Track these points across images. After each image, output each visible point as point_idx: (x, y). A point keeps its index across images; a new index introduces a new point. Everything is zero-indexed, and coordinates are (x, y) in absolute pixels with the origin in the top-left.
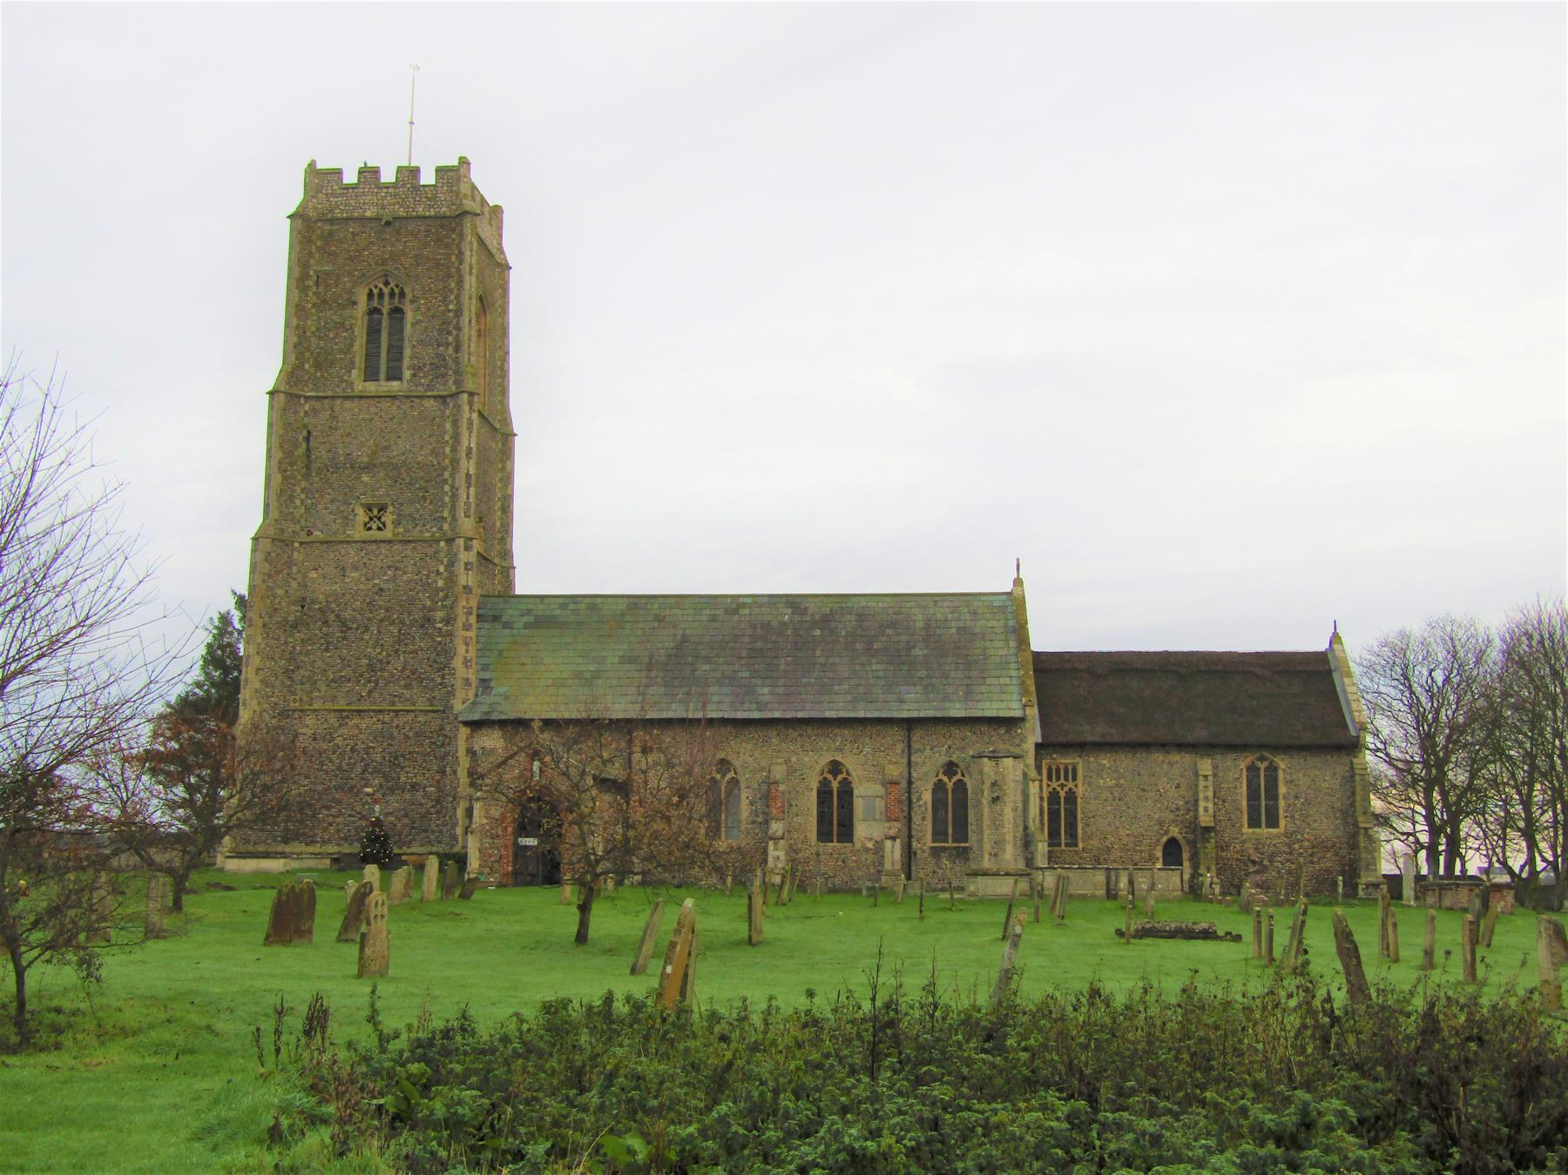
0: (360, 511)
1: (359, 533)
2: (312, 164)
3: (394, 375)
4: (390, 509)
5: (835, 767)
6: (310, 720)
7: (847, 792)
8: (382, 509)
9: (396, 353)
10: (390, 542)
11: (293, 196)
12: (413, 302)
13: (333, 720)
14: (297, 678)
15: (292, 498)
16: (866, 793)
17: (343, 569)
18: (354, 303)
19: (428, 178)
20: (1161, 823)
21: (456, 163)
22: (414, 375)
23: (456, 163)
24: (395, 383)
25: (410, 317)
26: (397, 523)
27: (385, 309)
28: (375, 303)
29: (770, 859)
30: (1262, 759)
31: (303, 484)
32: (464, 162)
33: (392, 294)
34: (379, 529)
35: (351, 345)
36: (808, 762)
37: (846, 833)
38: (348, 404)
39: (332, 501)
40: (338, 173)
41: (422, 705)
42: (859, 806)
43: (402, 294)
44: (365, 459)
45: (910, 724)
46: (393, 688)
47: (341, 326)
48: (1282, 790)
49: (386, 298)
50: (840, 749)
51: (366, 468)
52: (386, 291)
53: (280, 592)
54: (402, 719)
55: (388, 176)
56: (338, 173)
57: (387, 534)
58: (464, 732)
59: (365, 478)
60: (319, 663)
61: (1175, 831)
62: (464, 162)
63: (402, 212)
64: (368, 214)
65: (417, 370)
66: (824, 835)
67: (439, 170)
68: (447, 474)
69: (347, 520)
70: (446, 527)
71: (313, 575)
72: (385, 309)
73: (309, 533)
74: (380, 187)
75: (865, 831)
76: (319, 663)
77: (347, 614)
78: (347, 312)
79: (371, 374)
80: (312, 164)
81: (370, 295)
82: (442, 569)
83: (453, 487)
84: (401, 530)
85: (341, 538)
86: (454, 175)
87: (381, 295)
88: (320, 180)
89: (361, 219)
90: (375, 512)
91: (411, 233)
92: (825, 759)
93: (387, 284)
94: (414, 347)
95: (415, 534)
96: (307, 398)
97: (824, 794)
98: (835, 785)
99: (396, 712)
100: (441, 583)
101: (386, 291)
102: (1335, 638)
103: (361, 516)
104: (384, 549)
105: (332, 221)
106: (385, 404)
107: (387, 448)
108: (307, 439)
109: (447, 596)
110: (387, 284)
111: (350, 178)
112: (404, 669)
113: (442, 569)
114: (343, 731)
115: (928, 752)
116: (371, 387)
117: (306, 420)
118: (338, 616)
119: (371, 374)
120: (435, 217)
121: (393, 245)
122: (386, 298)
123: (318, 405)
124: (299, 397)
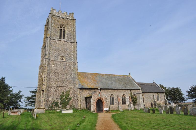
0: (60, 57)
1: (60, 60)
5: (124, 95)
6: (53, 88)
7: (125, 98)
8: (63, 57)
9: (64, 35)
13: (57, 88)
15: (50, 53)
16: (127, 98)
24: (64, 40)
25: (66, 31)
26: (65, 59)
33: (63, 28)
36: (121, 94)
37: (125, 104)
38: (58, 41)
41: (70, 86)
42: (126, 100)
43: (65, 28)
46: (66, 83)
47: (56, 30)
52: (63, 27)
57: (64, 61)
58: (79, 90)
59: (61, 52)
60: (54, 79)
61: (152, 102)
62: (73, 13)
63: (65, 17)
66: (123, 104)
68: (73, 53)
69: (58, 58)
71: (53, 65)
75: (128, 103)
77: (58, 72)
79: (60, 38)
81: (60, 27)
83: (74, 55)
85: (57, 60)
87: (62, 27)
90: (62, 57)
92: (123, 94)
95: (68, 61)
97: (123, 98)
100: (72, 68)
101: (63, 27)
104: (64, 62)
110: (63, 26)
114: (59, 90)
123: (53, 40)
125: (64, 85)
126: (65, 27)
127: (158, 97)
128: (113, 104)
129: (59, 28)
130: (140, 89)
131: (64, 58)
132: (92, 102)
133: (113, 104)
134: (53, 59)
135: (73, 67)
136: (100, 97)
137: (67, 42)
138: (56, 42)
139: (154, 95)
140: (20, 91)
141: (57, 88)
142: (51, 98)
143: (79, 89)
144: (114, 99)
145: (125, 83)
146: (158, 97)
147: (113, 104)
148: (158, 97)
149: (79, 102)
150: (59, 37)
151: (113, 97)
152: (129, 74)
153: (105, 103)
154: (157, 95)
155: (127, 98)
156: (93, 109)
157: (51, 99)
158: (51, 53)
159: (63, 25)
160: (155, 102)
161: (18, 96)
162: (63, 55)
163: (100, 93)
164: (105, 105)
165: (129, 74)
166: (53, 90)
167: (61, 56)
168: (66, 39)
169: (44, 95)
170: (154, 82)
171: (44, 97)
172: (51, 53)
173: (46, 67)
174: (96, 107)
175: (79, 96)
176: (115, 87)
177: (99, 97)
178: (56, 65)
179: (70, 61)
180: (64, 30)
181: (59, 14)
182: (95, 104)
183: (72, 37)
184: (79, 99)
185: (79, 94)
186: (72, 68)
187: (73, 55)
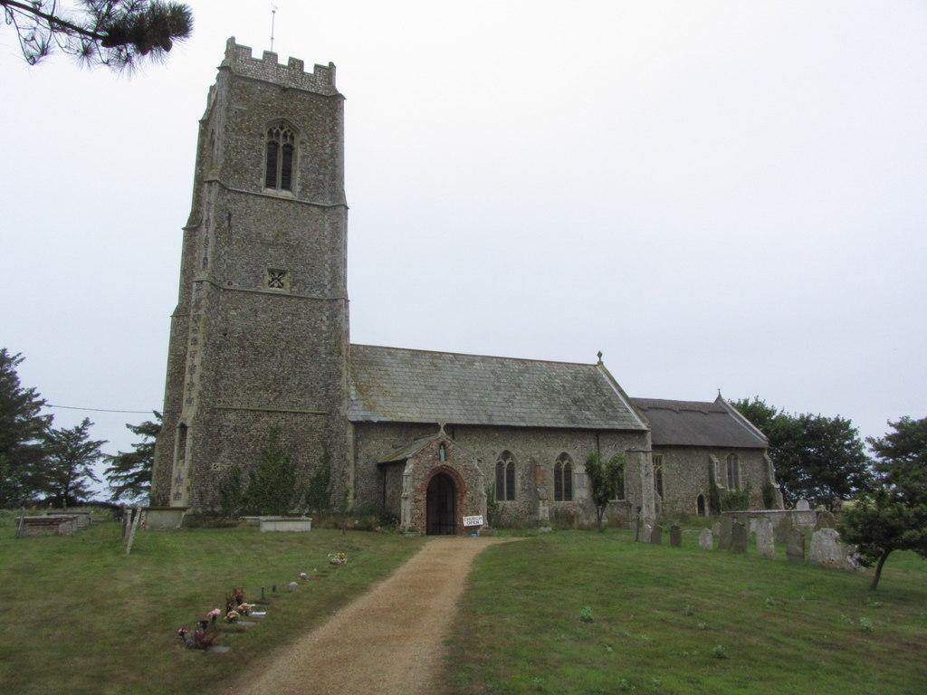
0: (266, 272)
2: (231, 41)
3: (287, 185)
4: (289, 274)
5: (564, 456)
6: (231, 416)
7: (569, 471)
8: (282, 273)
9: (287, 172)
10: (288, 296)
11: (219, 57)
12: (302, 143)
14: (221, 386)
16: (579, 469)
17: (256, 311)
18: (262, 135)
19: (309, 69)
20: (697, 486)
21: (327, 65)
22: (303, 189)
23: (327, 65)
25: (299, 152)
26: (293, 284)
27: (281, 145)
28: (274, 139)
29: (541, 512)
30: (733, 454)
31: (226, 249)
32: (332, 65)
33: (285, 136)
34: (279, 287)
35: (259, 163)
36: (550, 453)
37: (569, 496)
38: (258, 200)
39: (247, 264)
40: (249, 50)
41: (312, 409)
42: (576, 480)
43: (292, 138)
44: (272, 239)
45: (598, 433)
46: (293, 397)
47: (252, 148)
48: (740, 470)
49: (281, 137)
50: (565, 446)
51: (270, 245)
52: (282, 132)
53: (213, 322)
54: (299, 419)
55: (283, 61)
56: (249, 50)
57: (287, 292)
60: (238, 376)
62: (332, 65)
63: (293, 85)
64: (271, 81)
65: (305, 187)
67: (317, 67)
68: (326, 257)
70: (326, 291)
72: (281, 145)
73: (230, 284)
74: (279, 66)
76: (238, 376)
77: (258, 343)
78: (257, 140)
80: (231, 41)
81: (270, 133)
82: (325, 318)
84: (296, 290)
85: (253, 290)
86: (327, 72)
87: (278, 134)
88: (235, 51)
89: (268, 84)
91: (300, 100)
92: (559, 452)
93: (282, 128)
94: (302, 171)
95: (305, 294)
96: (229, 190)
97: (557, 472)
98: (563, 466)
99: (295, 414)
102: (719, 398)
103: (268, 278)
104: (284, 300)
105: (246, 79)
106: (285, 205)
107: (285, 234)
108: (229, 219)
109: (328, 338)
111: (257, 54)
112: (300, 384)
113: (325, 318)
115: (606, 448)
116: (270, 192)
117: (228, 206)
118: (252, 344)
119: (271, 183)
120: (316, 95)
121: (287, 104)
122: (281, 137)
124: (225, 188)
125: (283, 405)
126: (295, 135)
127: (732, 473)
128: (511, 496)
129: (265, 140)
130: (641, 433)
131: (286, 277)
132: (405, 484)
133: (511, 496)
134: (235, 285)
135: (327, 323)
136: (449, 463)
137: (299, 208)
138: (251, 202)
139: (711, 461)
140: (86, 423)
141: (250, 416)
142: (218, 464)
143: (353, 423)
144: (518, 474)
145: (575, 402)
146: (736, 473)
147: (508, 499)
148: (732, 473)
149: (350, 484)
150: (263, 181)
151: (511, 465)
152: (600, 355)
153: (469, 494)
154: (729, 459)
155: (579, 469)
156: (409, 519)
157: (219, 469)
158: (226, 257)
159: (282, 123)
160: (713, 489)
161: (75, 448)
162: (282, 264)
163: (444, 446)
164: (465, 501)
165: (600, 355)
166: (232, 425)
167: (272, 272)
168: (298, 188)
169: (188, 449)
170: (719, 398)
171: (188, 456)
172: (226, 257)
173: (202, 319)
174: (424, 511)
175: (350, 456)
176: (522, 419)
177: (438, 464)
178: (243, 310)
179: (314, 295)
180: (289, 151)
181: (264, 68)
182: (422, 497)
183: (327, 179)
184: (350, 471)
185: (351, 449)
186: (324, 328)
187: (327, 266)
